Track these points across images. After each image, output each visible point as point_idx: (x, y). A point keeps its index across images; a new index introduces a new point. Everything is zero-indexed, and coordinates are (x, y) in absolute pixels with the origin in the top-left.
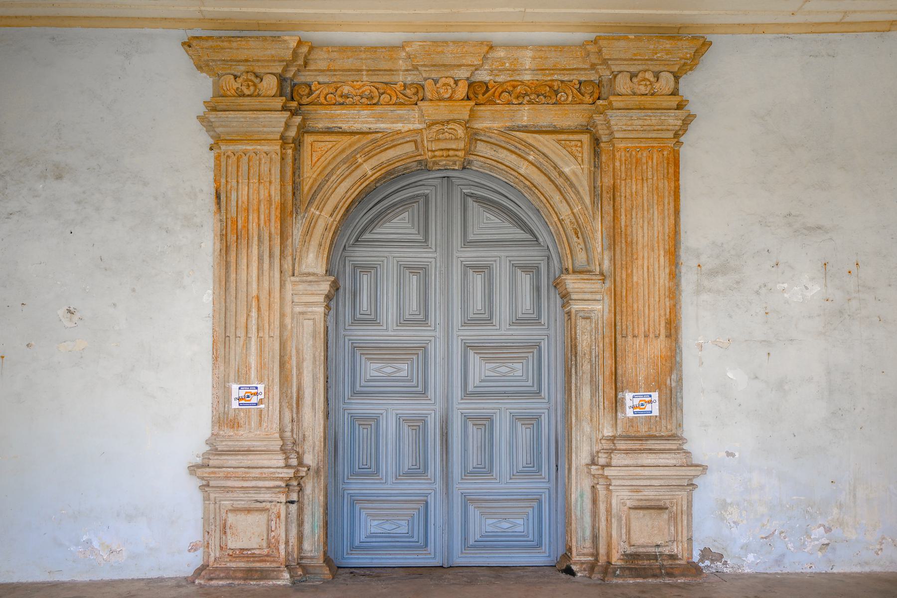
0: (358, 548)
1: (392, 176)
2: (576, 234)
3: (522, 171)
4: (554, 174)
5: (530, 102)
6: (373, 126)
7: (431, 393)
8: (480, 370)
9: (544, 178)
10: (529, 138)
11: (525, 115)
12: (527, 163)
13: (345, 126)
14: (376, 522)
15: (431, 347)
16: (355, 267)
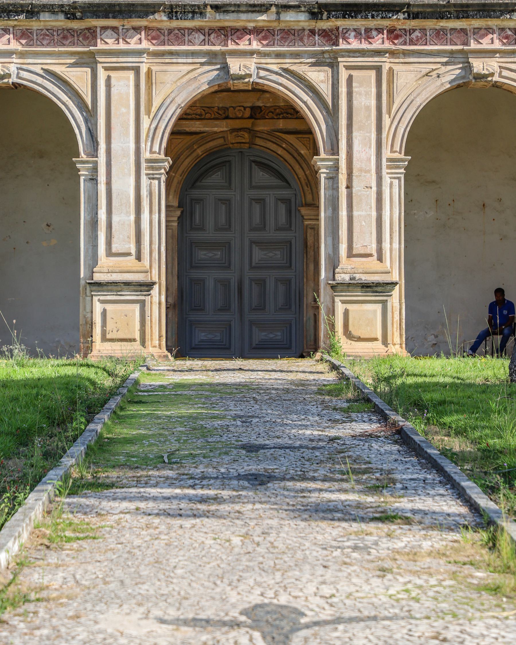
0: (194, 348)
1: (212, 154)
2: (307, 185)
3: (279, 153)
4: (296, 155)
5: (284, 118)
6: (202, 129)
7: (232, 267)
8: (258, 254)
9: (290, 156)
10: (284, 136)
11: (281, 124)
12: (281, 149)
13: (187, 129)
14: (203, 334)
15: (233, 243)
16: (192, 200)
